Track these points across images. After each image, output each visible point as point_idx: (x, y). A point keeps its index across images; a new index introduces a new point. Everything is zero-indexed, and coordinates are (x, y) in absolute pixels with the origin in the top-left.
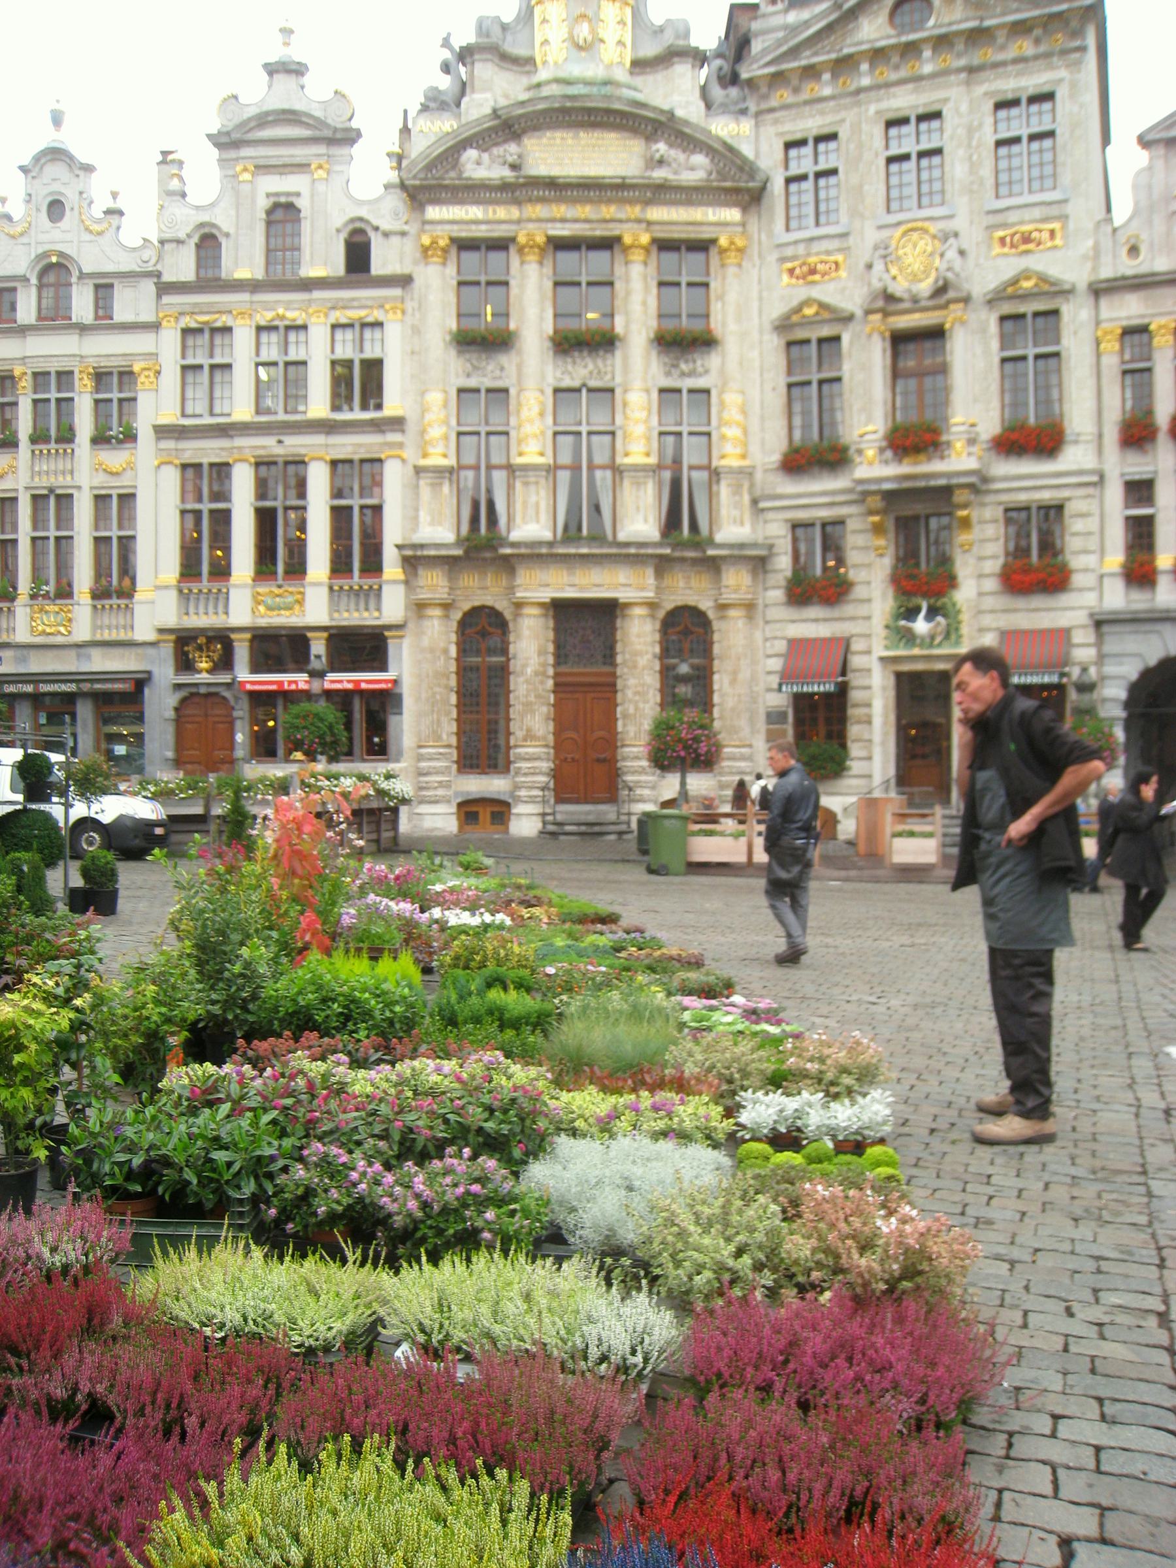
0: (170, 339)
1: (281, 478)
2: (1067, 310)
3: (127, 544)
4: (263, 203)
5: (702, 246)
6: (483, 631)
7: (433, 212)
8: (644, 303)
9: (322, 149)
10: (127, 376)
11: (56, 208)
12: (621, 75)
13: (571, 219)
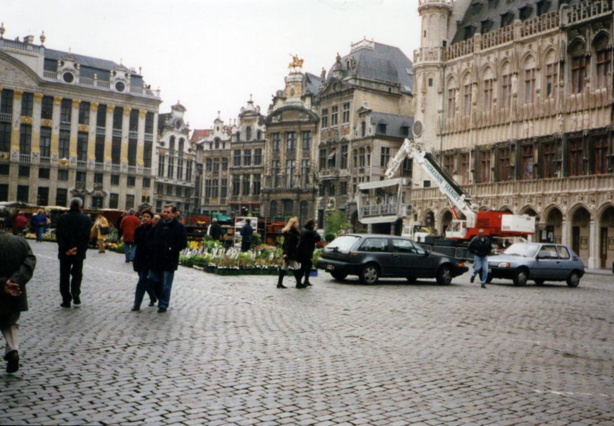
0: (232, 153)
10: (227, 159)
11: (218, 129)
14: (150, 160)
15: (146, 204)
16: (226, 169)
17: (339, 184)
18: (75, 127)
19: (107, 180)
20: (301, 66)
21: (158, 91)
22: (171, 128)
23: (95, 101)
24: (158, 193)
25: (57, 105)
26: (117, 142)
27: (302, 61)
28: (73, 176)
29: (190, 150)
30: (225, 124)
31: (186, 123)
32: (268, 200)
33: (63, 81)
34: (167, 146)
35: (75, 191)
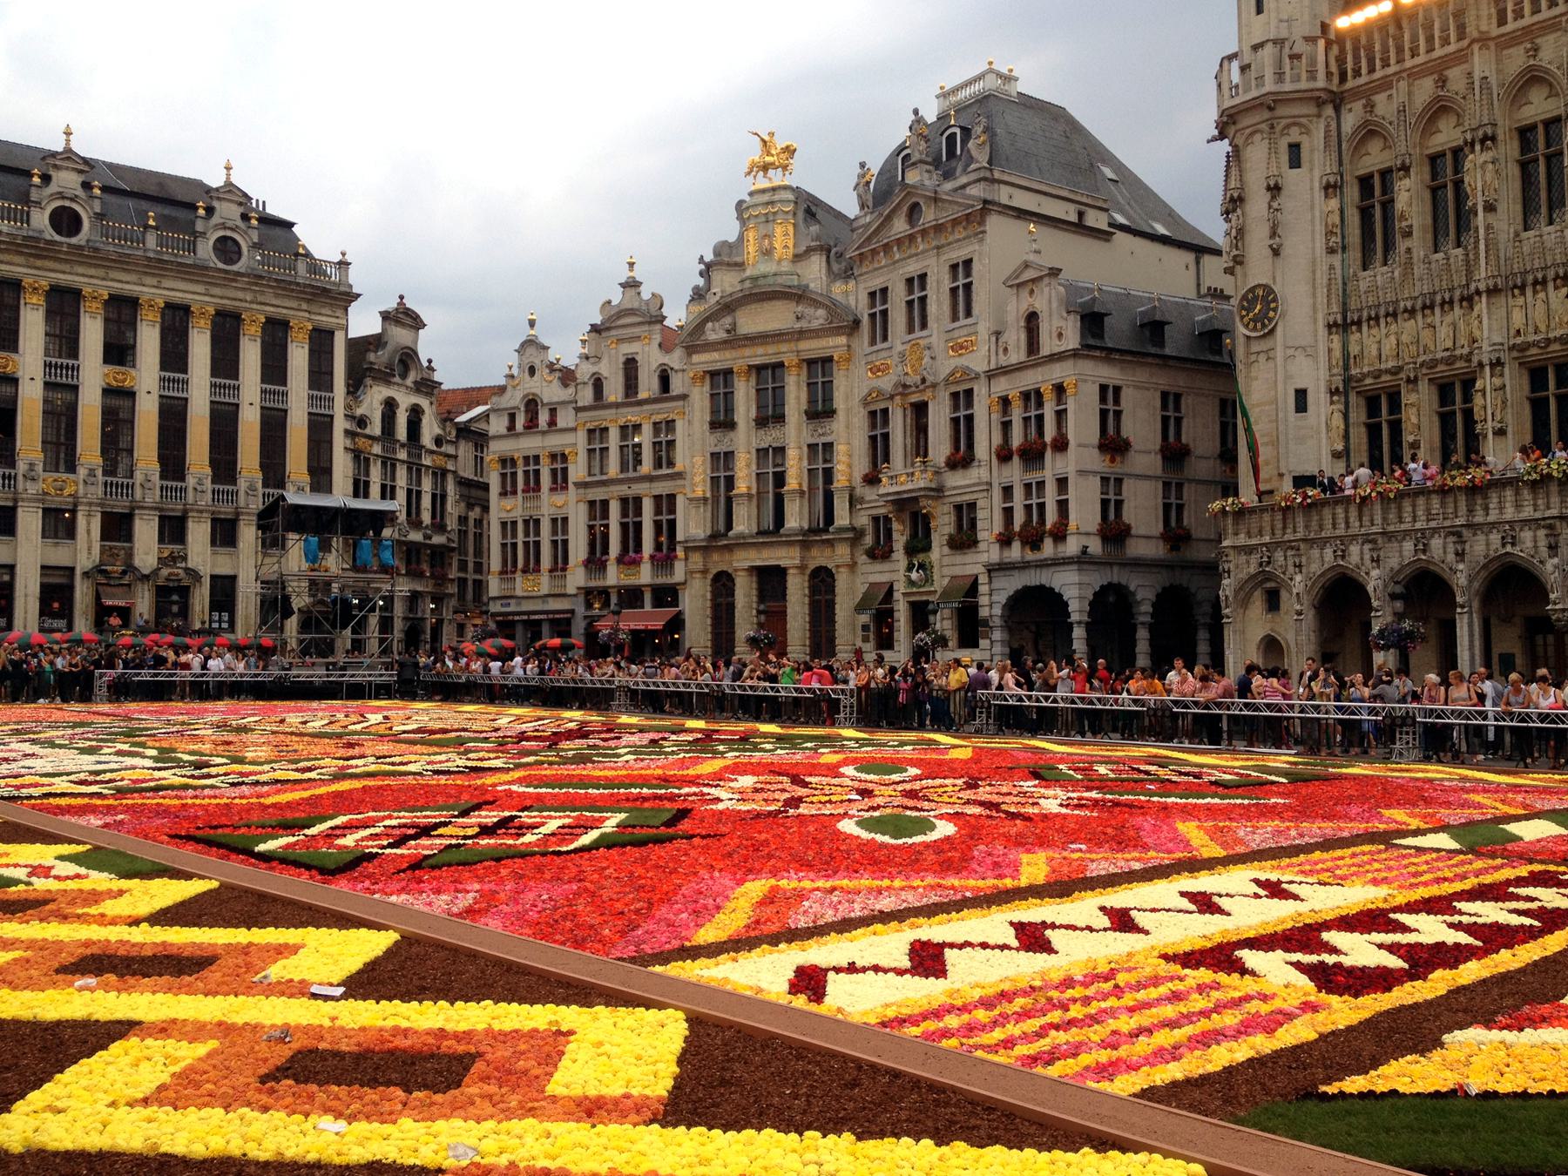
0: (581, 438)
1: (631, 505)
4: (622, 359)
5: (830, 359)
6: (723, 584)
7: (696, 358)
8: (798, 398)
9: (646, 328)
11: (532, 371)
12: (786, 267)
14: (328, 471)
17: (946, 509)
18: (93, 374)
19: (199, 533)
20: (785, 168)
21: (343, 264)
22: (385, 377)
23: (153, 292)
25: (36, 307)
26: (224, 422)
27: (790, 151)
28: (89, 527)
29: (438, 441)
30: (552, 356)
31: (425, 364)
32: (704, 572)
33: (50, 234)
34: (376, 428)
35: (99, 570)
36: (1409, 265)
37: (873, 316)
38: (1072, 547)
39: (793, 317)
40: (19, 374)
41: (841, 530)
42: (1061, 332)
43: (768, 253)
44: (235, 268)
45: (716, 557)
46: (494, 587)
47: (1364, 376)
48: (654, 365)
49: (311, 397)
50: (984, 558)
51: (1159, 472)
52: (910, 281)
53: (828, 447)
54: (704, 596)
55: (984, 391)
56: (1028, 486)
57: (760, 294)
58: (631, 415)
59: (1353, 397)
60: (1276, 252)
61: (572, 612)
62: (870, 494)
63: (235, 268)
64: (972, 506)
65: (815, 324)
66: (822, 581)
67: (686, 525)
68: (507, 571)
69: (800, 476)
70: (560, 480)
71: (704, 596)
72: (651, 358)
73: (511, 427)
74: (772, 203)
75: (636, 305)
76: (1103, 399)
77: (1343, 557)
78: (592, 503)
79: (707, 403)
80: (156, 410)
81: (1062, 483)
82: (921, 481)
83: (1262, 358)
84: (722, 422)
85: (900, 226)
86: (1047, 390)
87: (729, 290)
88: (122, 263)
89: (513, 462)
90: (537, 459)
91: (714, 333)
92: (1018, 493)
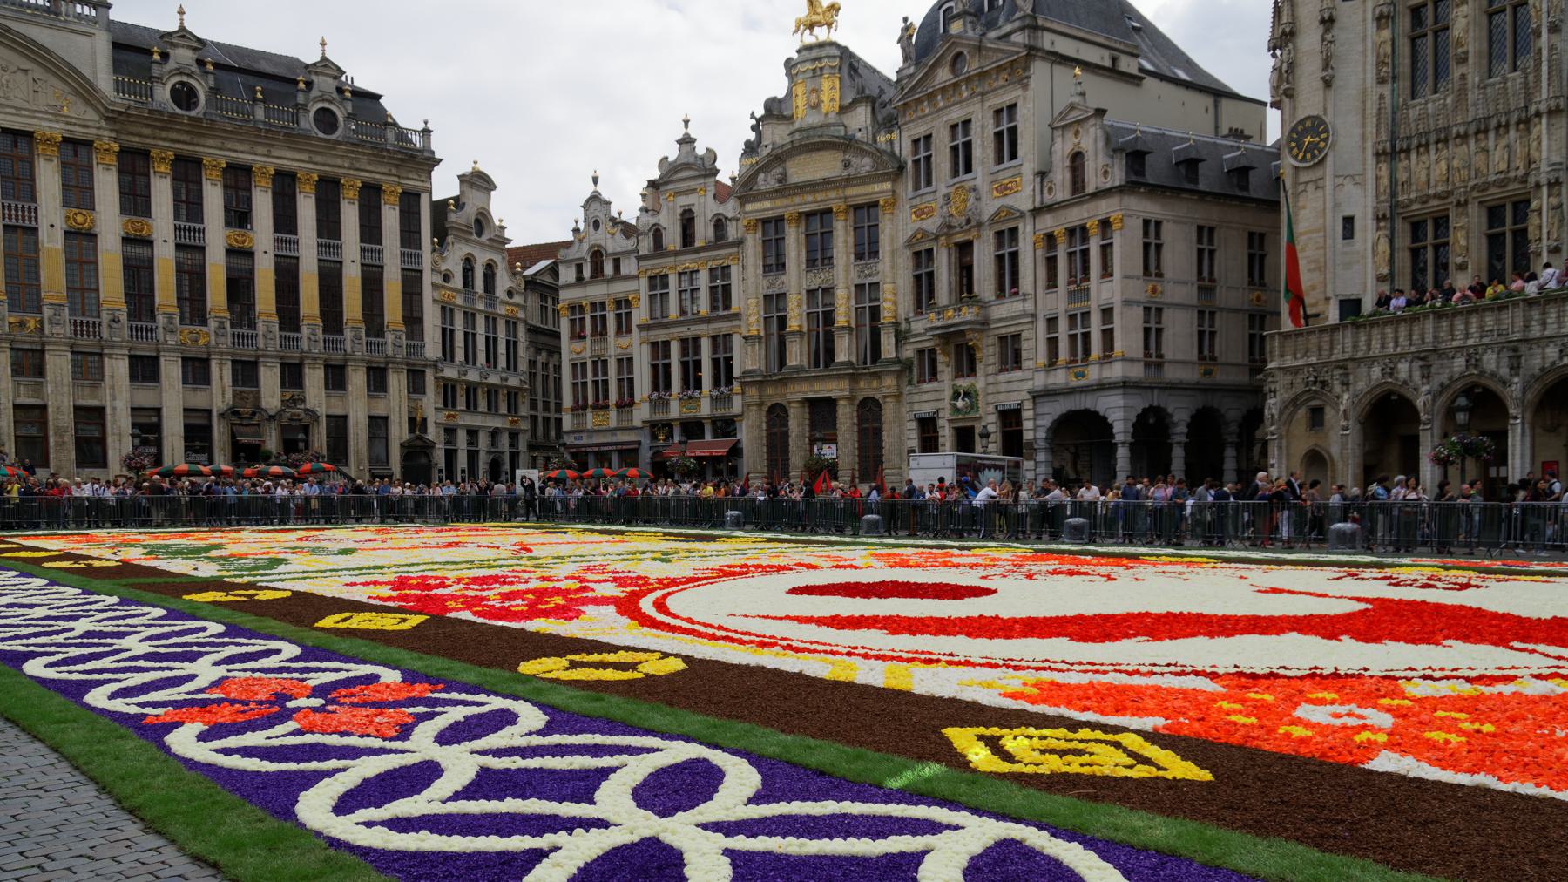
1: (690, 346)
2: (1021, 227)
3: (631, 381)
4: (679, 211)
5: (875, 204)
7: (749, 207)
10: (628, 303)
11: (596, 225)
12: (832, 119)
13: (809, 202)
14: (420, 321)
15: (419, 438)
16: (629, 331)
18: (216, 235)
22: (464, 233)
23: (265, 160)
24: (446, 404)
32: (760, 405)
34: (458, 282)
36: (1462, 91)
37: (916, 162)
38: (1116, 371)
39: (840, 165)
40: (154, 236)
41: (888, 361)
42: (1102, 171)
43: (816, 106)
44: (333, 137)
45: (770, 391)
46: (567, 423)
47: (1412, 202)
48: (710, 215)
49: (403, 254)
50: (1029, 385)
51: (1195, 302)
52: (954, 127)
53: (875, 286)
54: (760, 427)
55: (1029, 228)
56: (1072, 318)
57: (810, 144)
58: (688, 262)
59: (1399, 224)
60: (1328, 84)
61: (639, 443)
62: (918, 326)
63: (333, 137)
64: (1016, 337)
65: (863, 171)
66: (869, 410)
67: (743, 362)
68: (579, 408)
69: (848, 315)
70: (624, 326)
71: (760, 427)
72: (706, 208)
73: (580, 278)
74: (819, 59)
75: (691, 160)
76: (1146, 234)
77: (1391, 375)
78: (654, 345)
79: (760, 249)
80: (272, 268)
81: (1107, 313)
82: (969, 314)
83: (1311, 187)
84: (775, 264)
85: (944, 75)
86: (1092, 224)
87: (779, 142)
88: (236, 134)
89: (581, 308)
90: (603, 304)
91: (766, 182)
92: (1063, 325)
